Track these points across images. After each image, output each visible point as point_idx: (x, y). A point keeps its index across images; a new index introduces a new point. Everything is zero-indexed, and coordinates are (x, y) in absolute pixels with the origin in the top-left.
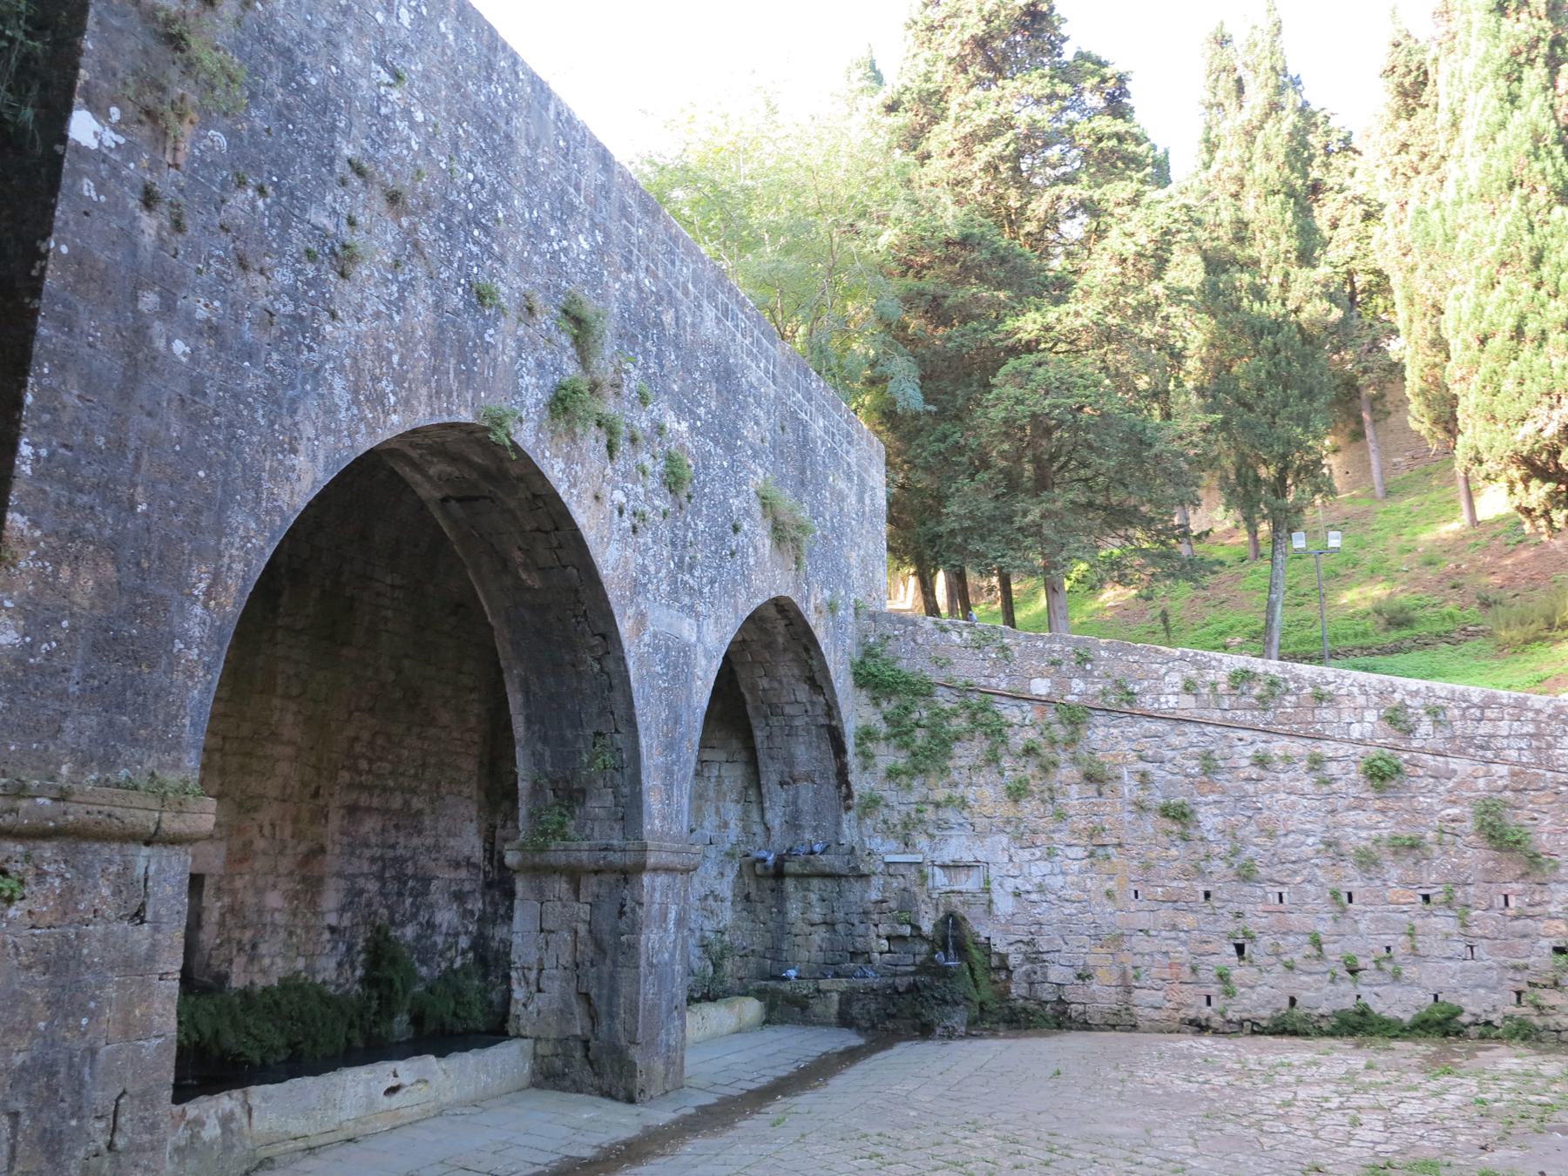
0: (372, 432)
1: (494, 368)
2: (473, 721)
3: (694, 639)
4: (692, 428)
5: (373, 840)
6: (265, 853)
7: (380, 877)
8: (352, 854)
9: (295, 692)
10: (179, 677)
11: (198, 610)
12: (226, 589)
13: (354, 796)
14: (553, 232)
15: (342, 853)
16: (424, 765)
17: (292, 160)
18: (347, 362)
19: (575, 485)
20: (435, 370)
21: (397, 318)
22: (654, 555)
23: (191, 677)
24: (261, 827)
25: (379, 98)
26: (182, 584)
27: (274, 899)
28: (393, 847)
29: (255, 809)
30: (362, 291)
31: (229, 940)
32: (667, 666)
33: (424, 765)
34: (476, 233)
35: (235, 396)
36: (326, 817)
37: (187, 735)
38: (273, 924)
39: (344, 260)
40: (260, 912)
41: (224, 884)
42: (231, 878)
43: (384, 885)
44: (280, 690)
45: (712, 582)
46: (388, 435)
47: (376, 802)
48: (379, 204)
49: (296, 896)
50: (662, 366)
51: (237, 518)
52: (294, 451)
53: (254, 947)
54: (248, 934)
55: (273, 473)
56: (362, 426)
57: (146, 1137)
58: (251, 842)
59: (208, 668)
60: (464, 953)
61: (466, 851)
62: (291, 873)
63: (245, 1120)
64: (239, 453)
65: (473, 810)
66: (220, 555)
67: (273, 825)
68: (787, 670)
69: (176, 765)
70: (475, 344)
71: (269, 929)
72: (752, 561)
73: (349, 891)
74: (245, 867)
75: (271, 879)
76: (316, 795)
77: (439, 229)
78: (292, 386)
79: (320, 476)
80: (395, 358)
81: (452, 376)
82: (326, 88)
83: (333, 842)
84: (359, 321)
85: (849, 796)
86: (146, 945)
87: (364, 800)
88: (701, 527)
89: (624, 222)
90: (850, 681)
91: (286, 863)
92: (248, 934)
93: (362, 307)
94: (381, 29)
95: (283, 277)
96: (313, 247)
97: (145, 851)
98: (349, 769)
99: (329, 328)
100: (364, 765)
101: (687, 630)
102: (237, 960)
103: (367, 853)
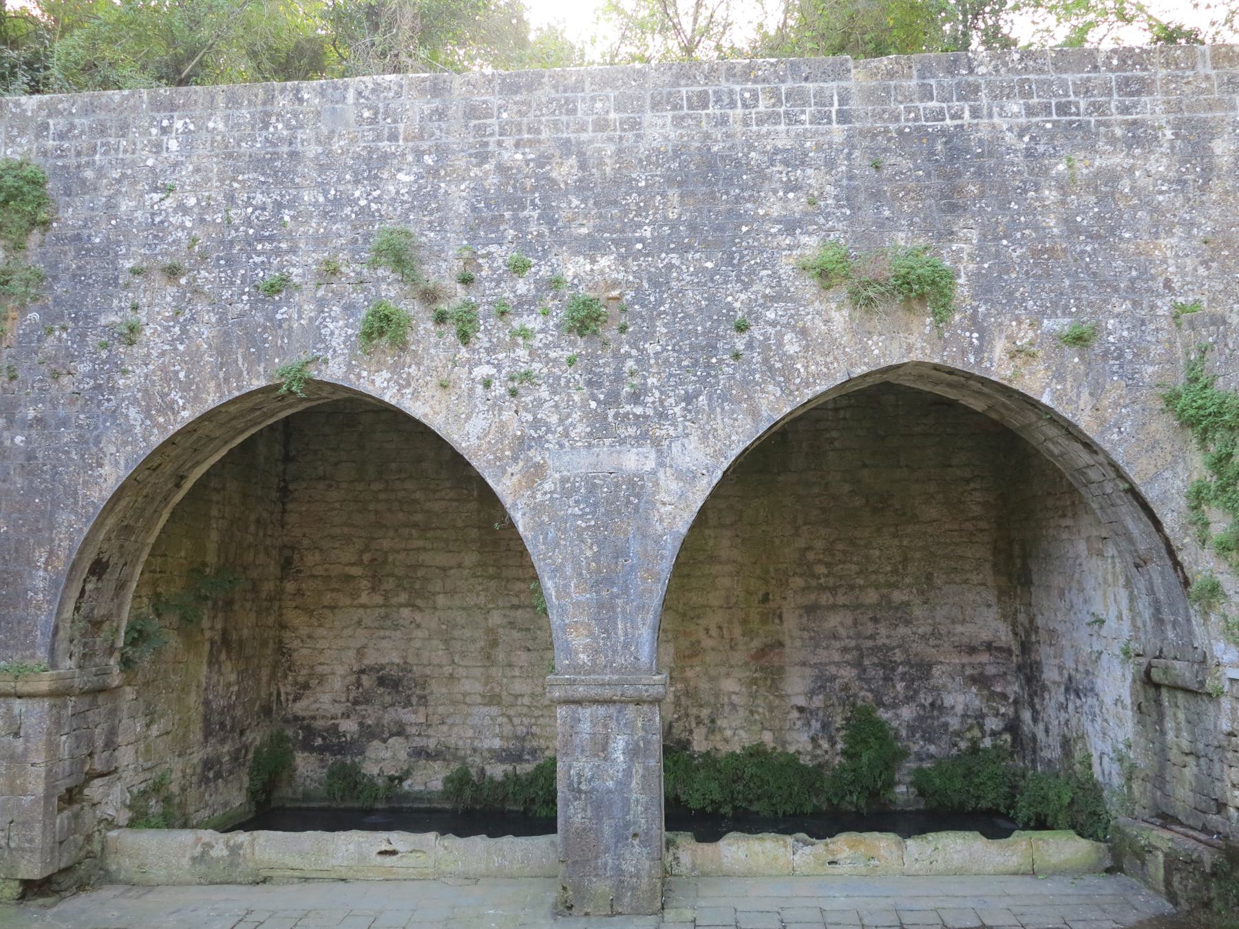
0: (163, 428)
1: (289, 337)
2: (976, 510)
3: (650, 464)
4: (622, 259)
5: (843, 632)
6: (713, 649)
7: (858, 664)
8: (817, 646)
9: (728, 521)
10: (32, 611)
11: (41, 573)
12: (58, 558)
13: (813, 597)
14: (357, 194)
16: (905, 560)
17: (86, 296)
18: (139, 395)
19: (408, 385)
21: (181, 348)
22: (562, 407)
23: (40, 609)
24: (707, 630)
25: (153, 214)
26: (30, 562)
28: (872, 637)
29: (699, 617)
30: (147, 346)
31: (687, 715)
34: (259, 247)
35: (56, 450)
36: (780, 617)
37: (39, 639)
39: (131, 334)
40: (717, 696)
41: (675, 674)
42: (683, 669)
43: (864, 671)
45: (688, 399)
46: (178, 427)
47: (841, 599)
48: (159, 280)
49: (754, 681)
50: (552, 222)
51: (63, 517)
52: (101, 465)
53: (713, 721)
54: (705, 713)
55: (86, 483)
56: (155, 431)
57: (27, 845)
58: (699, 642)
59: (50, 602)
60: (994, 734)
61: (985, 636)
62: (746, 664)
63: (249, 851)
64: (60, 482)
65: (991, 597)
66: (53, 540)
67: (720, 628)
68: (1052, 431)
69: (33, 656)
70: (265, 328)
71: (727, 709)
72: (792, 348)
75: (723, 670)
76: (765, 598)
77: (219, 266)
78: (96, 428)
79: (121, 473)
80: (182, 375)
81: (240, 362)
82: (108, 239)
83: (792, 637)
84: (147, 365)
85: (1186, 583)
86: (20, 750)
87: (825, 599)
88: (652, 348)
89: (474, 122)
90: (1162, 426)
91: (739, 657)
92: (705, 713)
93: (148, 355)
94: (152, 169)
95: (84, 368)
96: (105, 339)
97: (18, 701)
98: (801, 575)
99: (121, 382)
101: (635, 460)
102: (696, 731)
103: (837, 644)
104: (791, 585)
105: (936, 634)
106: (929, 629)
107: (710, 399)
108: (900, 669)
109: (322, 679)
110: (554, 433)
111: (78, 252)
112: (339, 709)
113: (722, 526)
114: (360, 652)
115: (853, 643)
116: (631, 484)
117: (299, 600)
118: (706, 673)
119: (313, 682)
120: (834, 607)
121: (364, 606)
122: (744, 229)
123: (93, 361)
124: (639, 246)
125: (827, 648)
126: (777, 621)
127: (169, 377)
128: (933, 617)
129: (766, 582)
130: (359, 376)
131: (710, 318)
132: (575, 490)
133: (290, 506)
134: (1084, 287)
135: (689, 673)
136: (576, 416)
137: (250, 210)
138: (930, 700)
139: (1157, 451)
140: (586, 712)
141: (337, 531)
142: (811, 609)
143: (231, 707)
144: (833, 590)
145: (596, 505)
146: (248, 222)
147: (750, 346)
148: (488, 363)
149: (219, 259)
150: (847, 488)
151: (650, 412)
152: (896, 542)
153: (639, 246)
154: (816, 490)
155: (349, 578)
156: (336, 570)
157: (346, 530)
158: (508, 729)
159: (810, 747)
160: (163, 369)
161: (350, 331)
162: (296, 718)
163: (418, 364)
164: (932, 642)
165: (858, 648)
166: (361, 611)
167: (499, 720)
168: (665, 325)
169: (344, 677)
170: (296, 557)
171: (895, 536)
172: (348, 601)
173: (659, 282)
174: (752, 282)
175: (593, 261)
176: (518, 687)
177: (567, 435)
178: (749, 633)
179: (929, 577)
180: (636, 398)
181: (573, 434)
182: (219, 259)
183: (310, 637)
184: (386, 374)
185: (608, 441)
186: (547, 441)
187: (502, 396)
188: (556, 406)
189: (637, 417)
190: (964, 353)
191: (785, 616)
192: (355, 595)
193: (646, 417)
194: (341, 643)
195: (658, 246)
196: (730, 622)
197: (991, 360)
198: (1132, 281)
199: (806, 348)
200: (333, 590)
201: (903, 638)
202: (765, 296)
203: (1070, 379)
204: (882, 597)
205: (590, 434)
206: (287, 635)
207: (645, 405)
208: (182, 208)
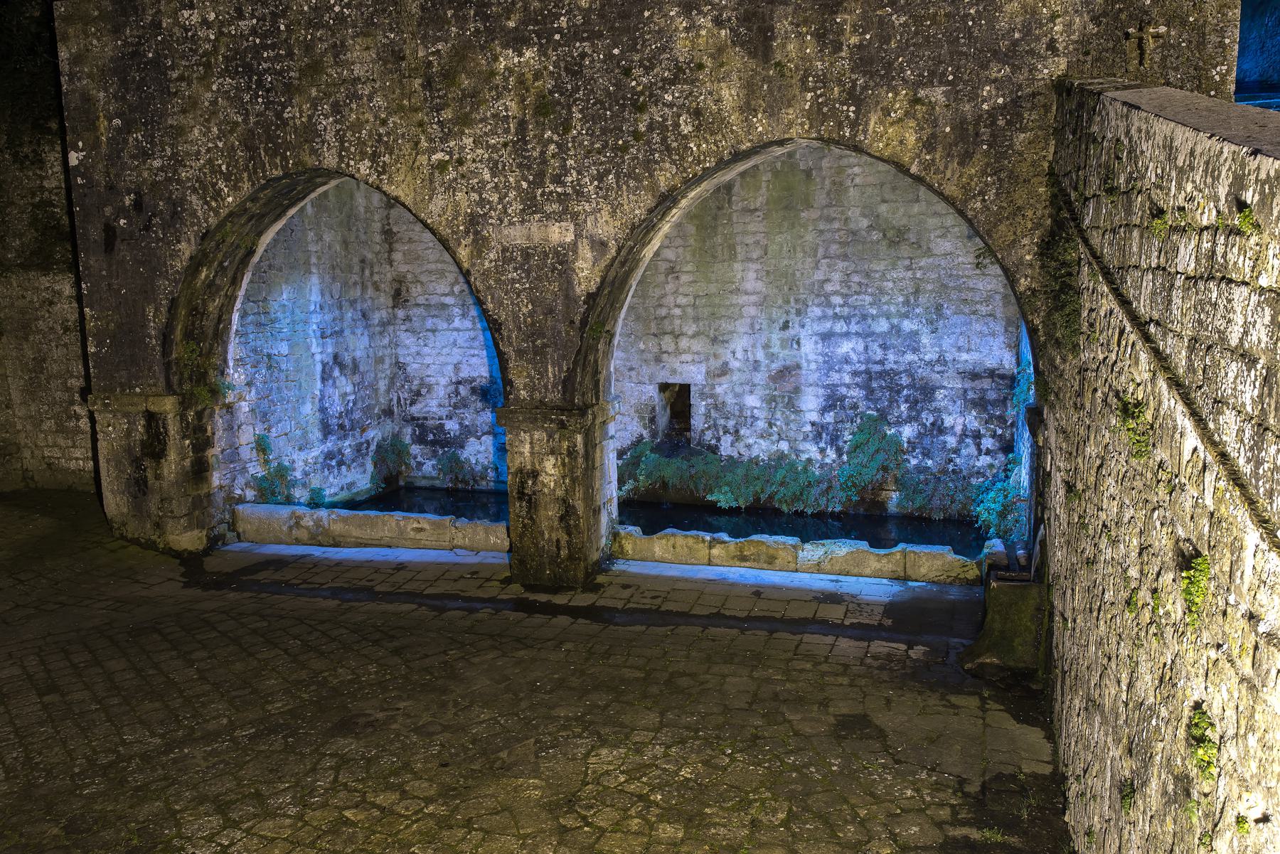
0: (217, 213)
3: (570, 238)
4: (542, 52)
5: (854, 357)
6: (739, 370)
13: (828, 325)
15: (818, 369)
16: (917, 292)
19: (384, 172)
20: (252, 158)
21: (220, 145)
24: (734, 353)
26: (144, 316)
29: (727, 342)
31: (715, 425)
32: (528, 272)
33: (917, 292)
36: (798, 343)
38: (753, 417)
40: (741, 410)
44: (739, 257)
45: (601, 177)
52: (179, 242)
53: (737, 431)
54: (731, 423)
55: (171, 255)
61: (990, 363)
65: (999, 327)
73: (829, 397)
74: (723, 379)
75: (747, 388)
80: (224, 167)
87: (840, 327)
93: (199, 152)
95: (157, 163)
98: (818, 305)
100: (837, 300)
101: (559, 233)
103: (847, 368)
104: (810, 314)
105: (941, 360)
106: (935, 357)
107: (617, 176)
108: (905, 392)
109: (430, 388)
110: (495, 210)
111: (139, 65)
112: (443, 412)
113: (749, 260)
114: (457, 367)
115: (863, 368)
116: (557, 253)
117: (408, 325)
118: (733, 390)
119: (424, 391)
120: (847, 335)
121: (457, 330)
122: (646, 14)
123: (162, 157)
124: (557, 37)
125: (839, 371)
126: (795, 346)
127: (216, 171)
128: (940, 346)
129: (787, 313)
130: (348, 165)
131: (618, 104)
132: (512, 259)
133: (397, 246)
134: (965, 54)
135: (719, 390)
136: (512, 194)
137: (255, 21)
138: (931, 419)
139: (1019, 219)
141: (433, 266)
142: (826, 337)
143: (349, 412)
144: (847, 319)
145: (528, 272)
146: (254, 31)
147: (651, 128)
148: (442, 150)
149: (237, 66)
150: (865, 223)
151: (569, 191)
152: (910, 274)
153: (557, 37)
154: (836, 225)
155: (444, 306)
156: (434, 300)
157: (439, 266)
159: (819, 457)
160: (210, 161)
161: (338, 127)
162: (413, 419)
163: (391, 154)
164: (937, 368)
165: (868, 372)
166: (455, 333)
168: (581, 111)
169: (446, 387)
170: (404, 289)
171: (908, 268)
172: (445, 326)
173: (574, 69)
174: (652, 67)
175: (521, 55)
177: (505, 212)
178: (772, 357)
179: (939, 308)
180: (558, 180)
181: (510, 211)
182: (237, 66)
183: (418, 354)
184: (367, 163)
185: (537, 217)
186: (491, 217)
187: (455, 179)
188: (496, 186)
189: (559, 194)
190: (840, 126)
191: (802, 342)
192: (449, 320)
193: (565, 194)
194: (442, 359)
195: (573, 35)
196: (754, 346)
197: (865, 132)
198: (1015, 43)
199: (698, 129)
200: (433, 316)
201: (909, 363)
202: (664, 80)
203: (940, 148)
204: (893, 327)
205: (523, 210)
206: (400, 351)
207: (563, 184)
208: (205, 23)
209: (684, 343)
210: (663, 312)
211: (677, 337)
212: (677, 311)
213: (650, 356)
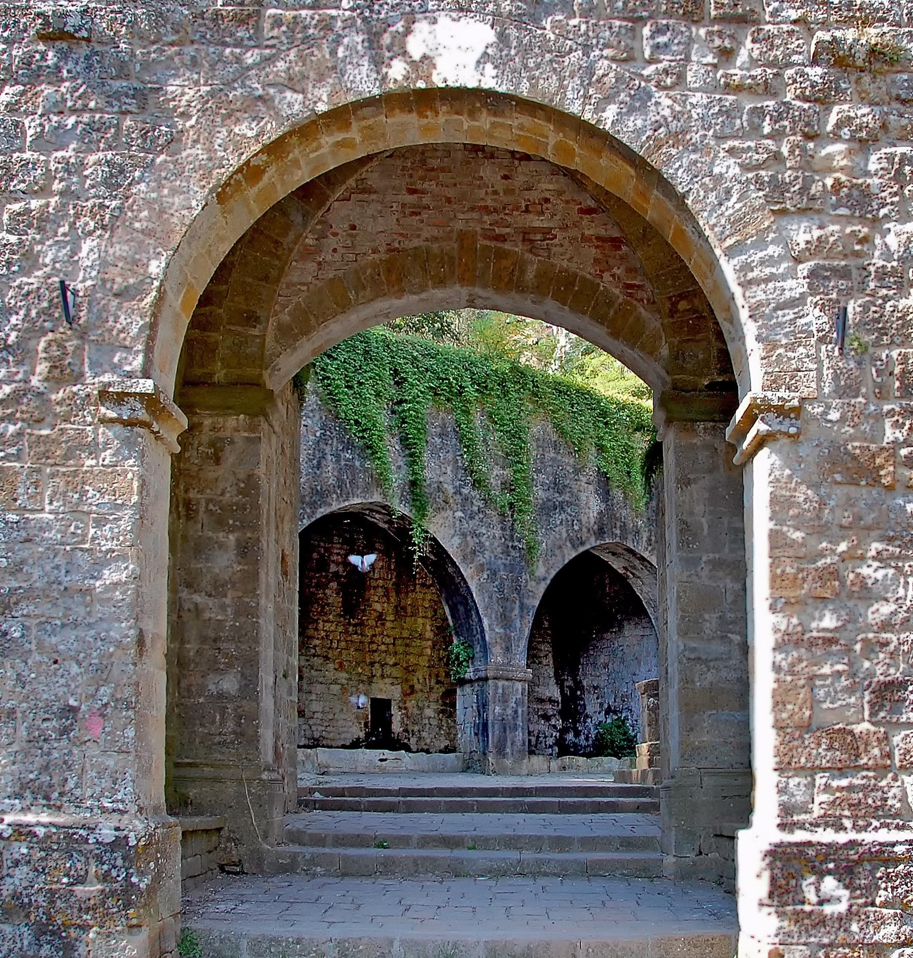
27: (429, 712)
91: (434, 696)
92: (416, 728)
135: (408, 704)
140: (500, 683)
158: (308, 733)
167: (304, 727)
176: (315, 706)
209: (388, 670)
210: (374, 647)
211: (382, 666)
212: (383, 647)
213: (365, 678)
